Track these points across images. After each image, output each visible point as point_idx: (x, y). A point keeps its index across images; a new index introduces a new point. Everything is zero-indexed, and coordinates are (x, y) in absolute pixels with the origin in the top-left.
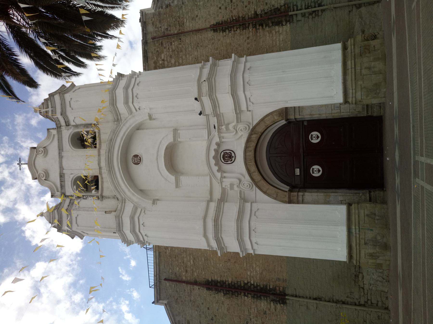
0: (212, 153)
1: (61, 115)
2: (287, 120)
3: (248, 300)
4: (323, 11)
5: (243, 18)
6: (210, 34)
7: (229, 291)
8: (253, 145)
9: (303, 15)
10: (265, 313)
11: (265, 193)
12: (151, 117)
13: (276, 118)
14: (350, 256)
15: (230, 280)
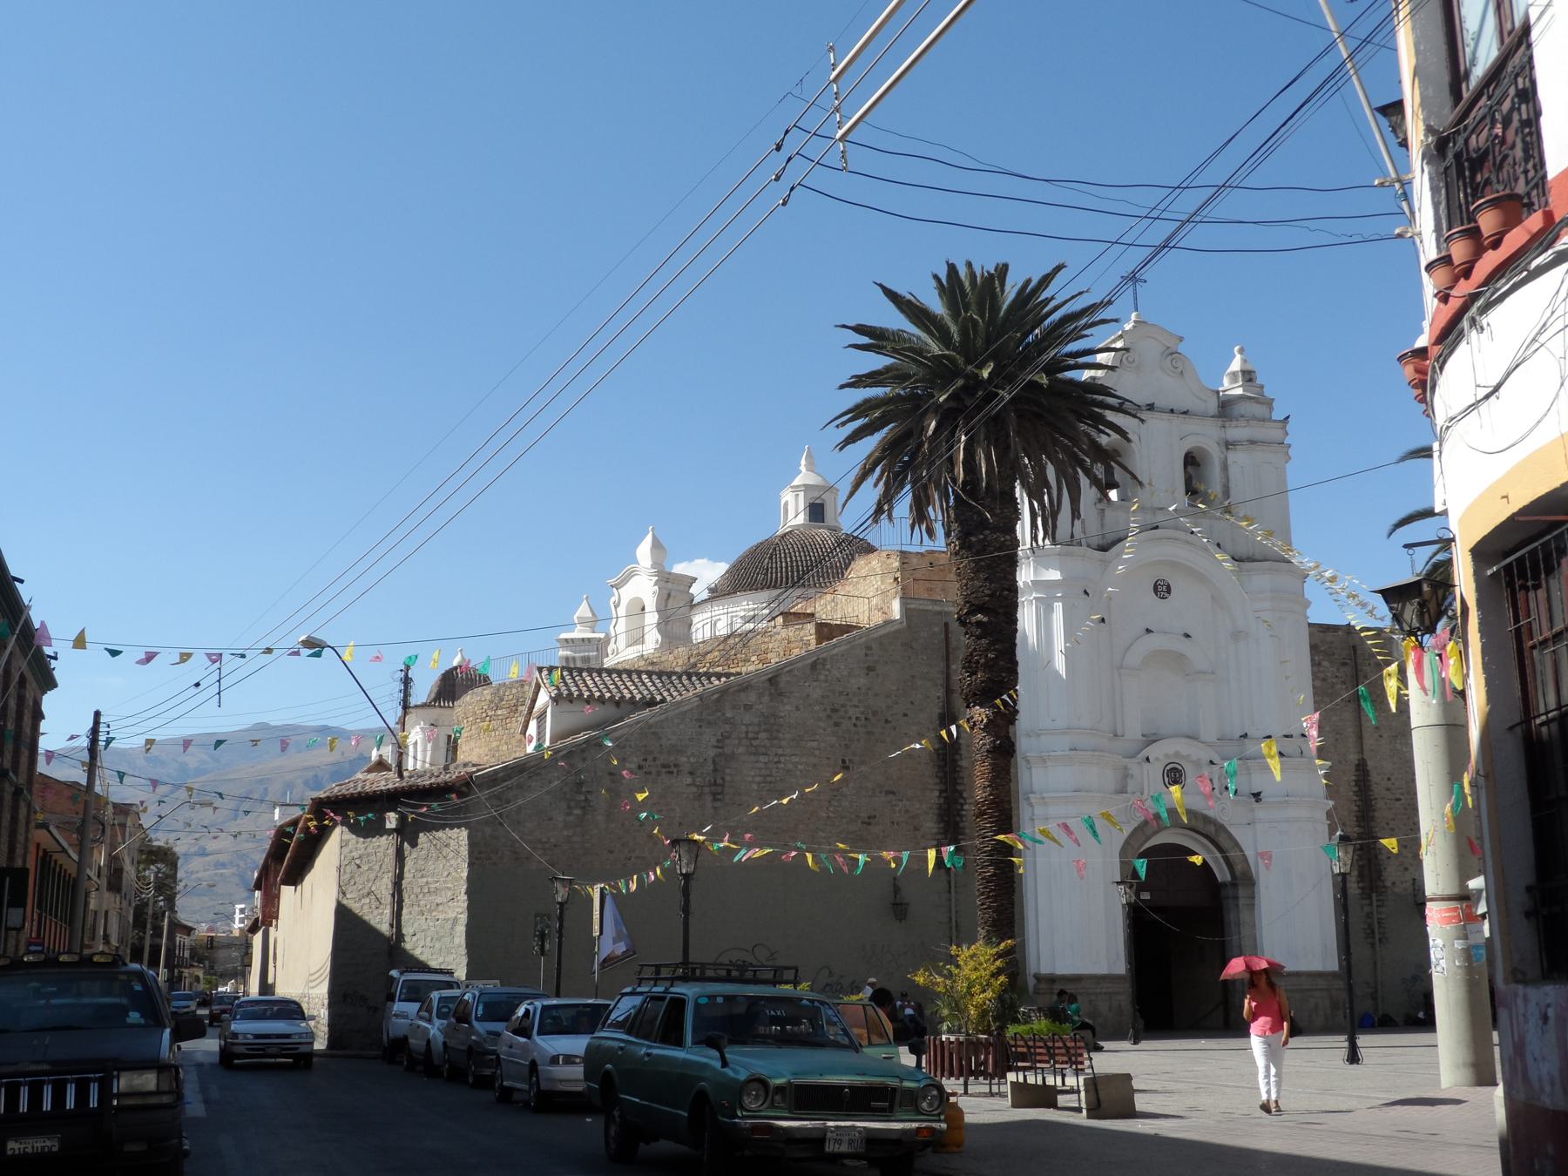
0: (1184, 753)
1: (1252, 442)
2: (1234, 884)
3: (934, 796)
4: (1373, 945)
5: (1373, 819)
6: (1353, 758)
7: (944, 760)
8: (1200, 825)
9: (1370, 915)
10: (916, 829)
11: (1127, 843)
12: (1237, 635)
13: (1238, 868)
14: (1052, 979)
15: (964, 763)
